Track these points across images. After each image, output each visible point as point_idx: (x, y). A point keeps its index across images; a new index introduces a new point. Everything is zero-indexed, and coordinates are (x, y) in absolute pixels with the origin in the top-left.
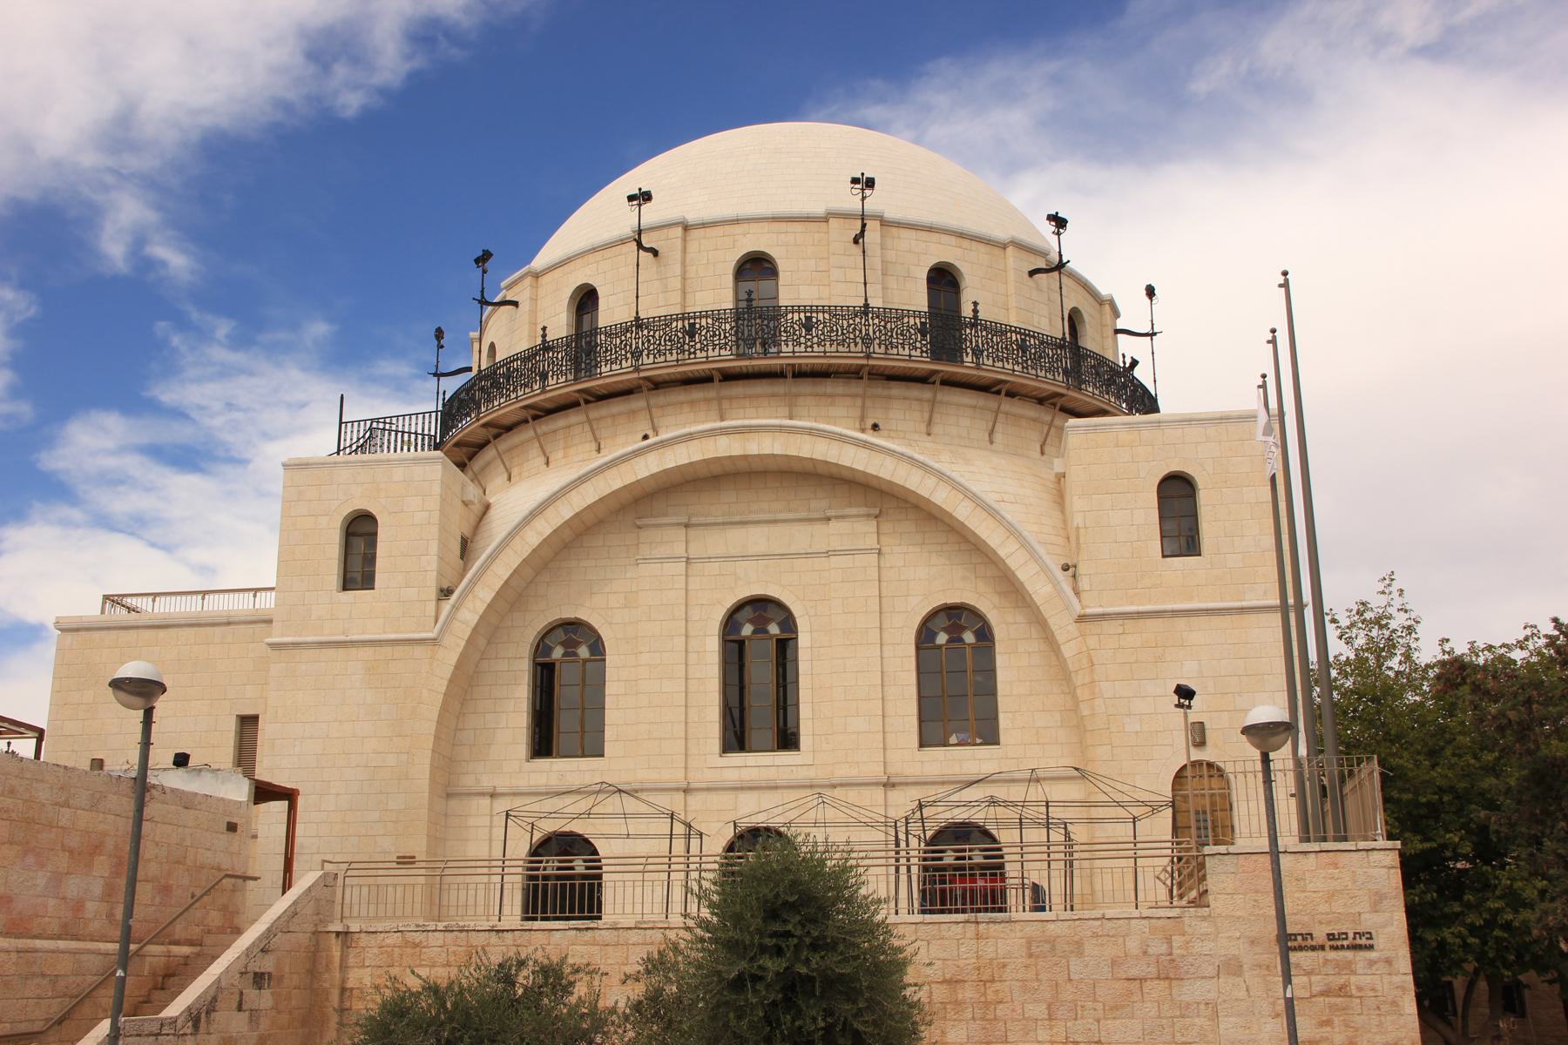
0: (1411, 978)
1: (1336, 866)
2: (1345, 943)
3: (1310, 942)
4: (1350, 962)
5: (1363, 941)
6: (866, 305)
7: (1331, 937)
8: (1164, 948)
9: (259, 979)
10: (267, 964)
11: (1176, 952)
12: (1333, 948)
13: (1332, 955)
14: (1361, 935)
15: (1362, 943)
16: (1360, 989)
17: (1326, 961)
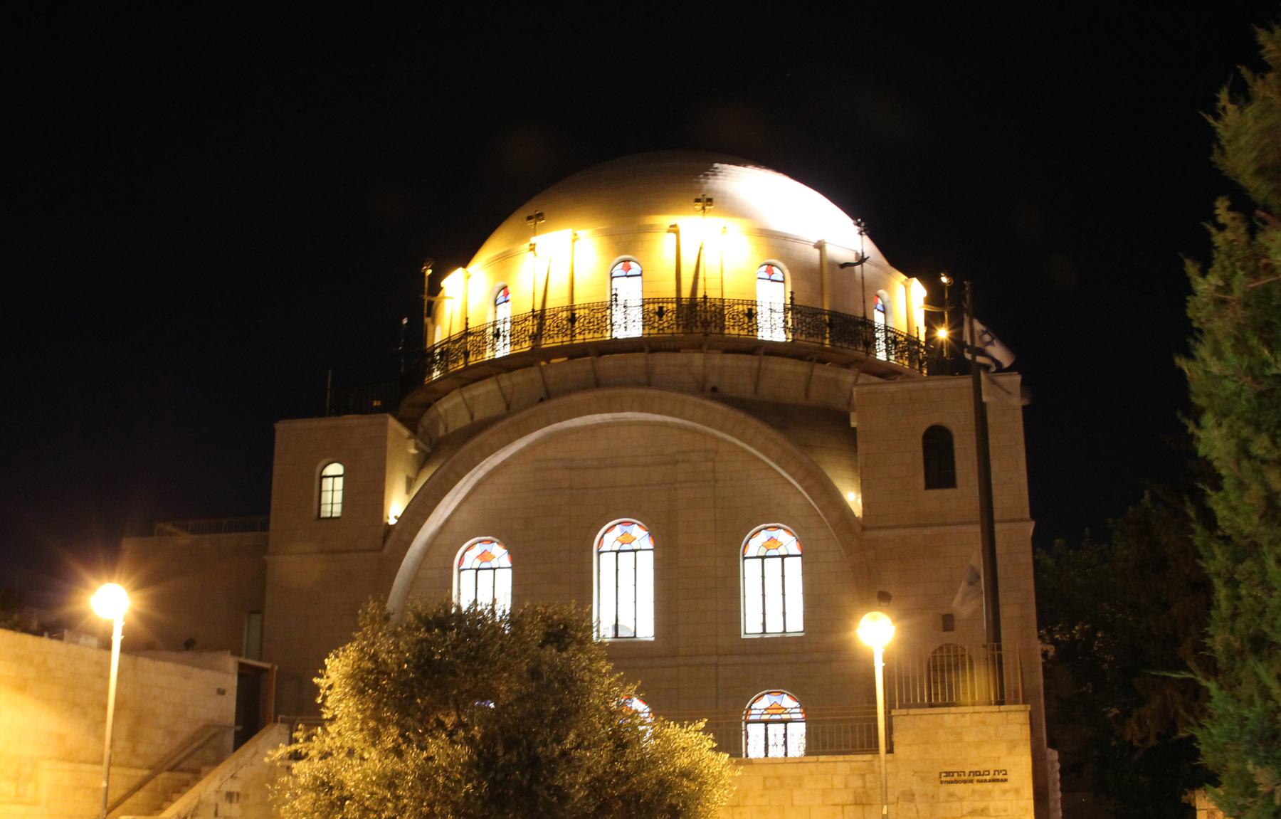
0: (1032, 802)
1: (984, 723)
2: (988, 778)
3: (963, 778)
4: (990, 792)
5: (1000, 777)
6: (705, 297)
7: (977, 773)
8: (859, 783)
9: (230, 796)
10: (235, 787)
11: (868, 785)
12: (980, 781)
13: (977, 786)
14: (999, 772)
15: (999, 777)
16: (996, 810)
17: (973, 792)
